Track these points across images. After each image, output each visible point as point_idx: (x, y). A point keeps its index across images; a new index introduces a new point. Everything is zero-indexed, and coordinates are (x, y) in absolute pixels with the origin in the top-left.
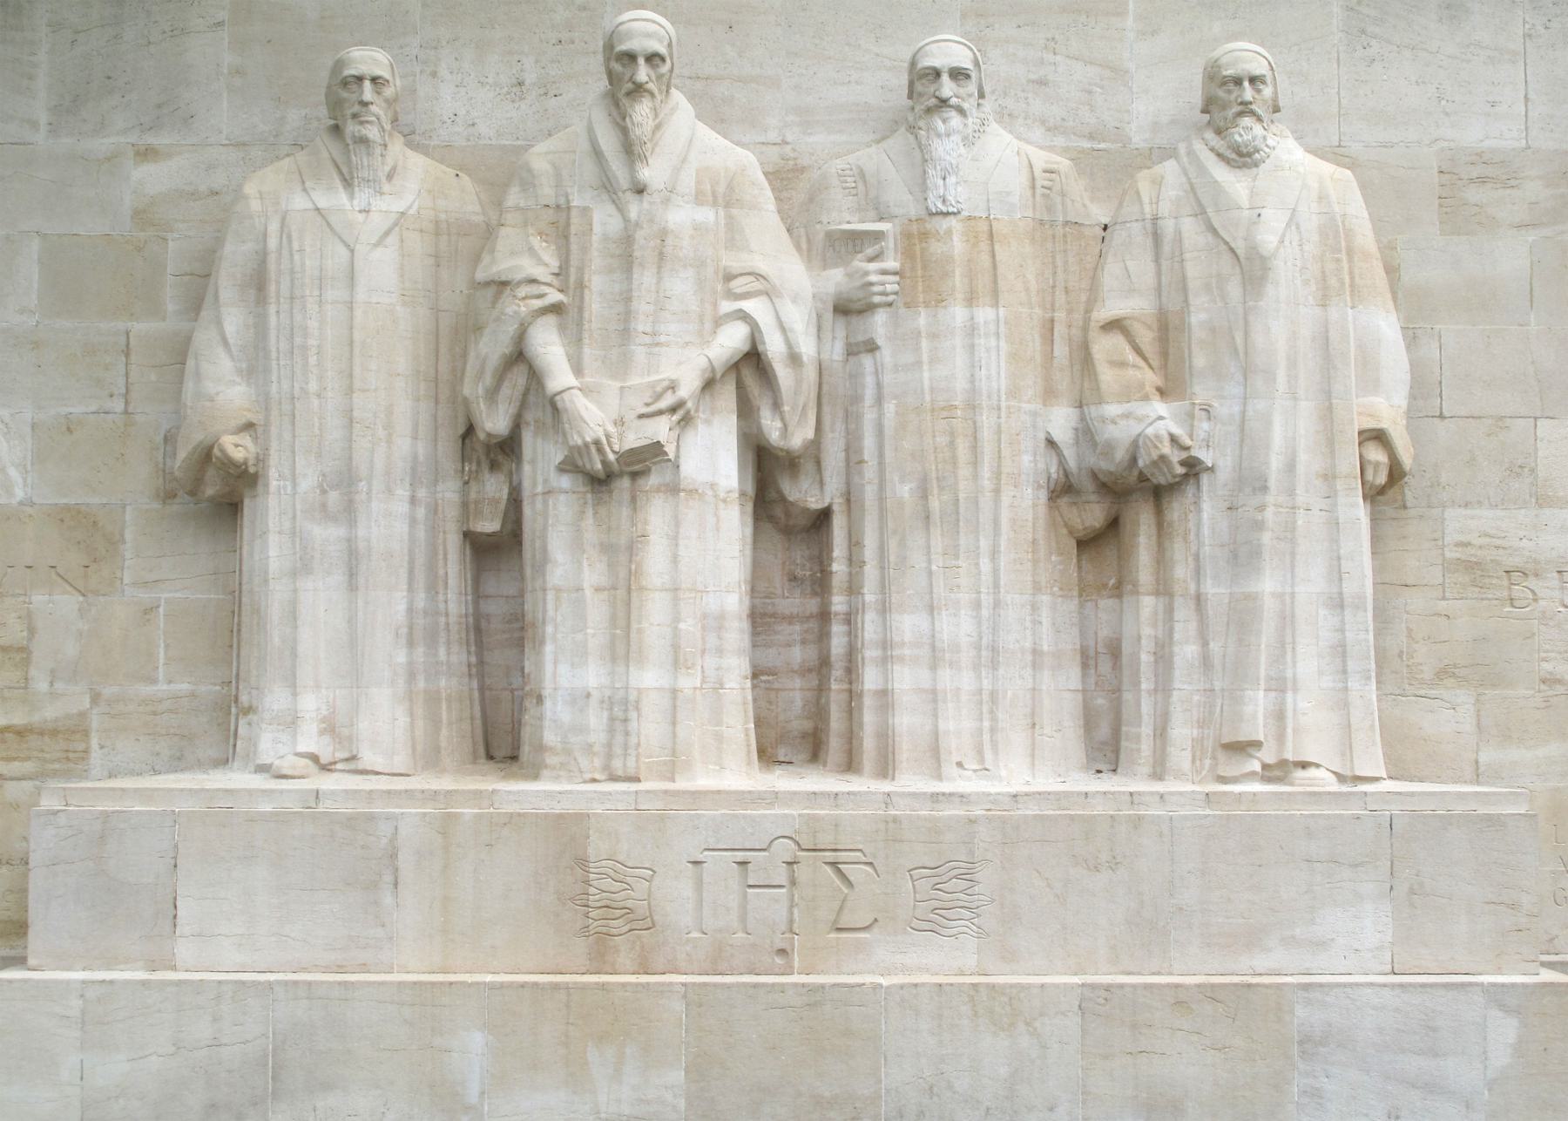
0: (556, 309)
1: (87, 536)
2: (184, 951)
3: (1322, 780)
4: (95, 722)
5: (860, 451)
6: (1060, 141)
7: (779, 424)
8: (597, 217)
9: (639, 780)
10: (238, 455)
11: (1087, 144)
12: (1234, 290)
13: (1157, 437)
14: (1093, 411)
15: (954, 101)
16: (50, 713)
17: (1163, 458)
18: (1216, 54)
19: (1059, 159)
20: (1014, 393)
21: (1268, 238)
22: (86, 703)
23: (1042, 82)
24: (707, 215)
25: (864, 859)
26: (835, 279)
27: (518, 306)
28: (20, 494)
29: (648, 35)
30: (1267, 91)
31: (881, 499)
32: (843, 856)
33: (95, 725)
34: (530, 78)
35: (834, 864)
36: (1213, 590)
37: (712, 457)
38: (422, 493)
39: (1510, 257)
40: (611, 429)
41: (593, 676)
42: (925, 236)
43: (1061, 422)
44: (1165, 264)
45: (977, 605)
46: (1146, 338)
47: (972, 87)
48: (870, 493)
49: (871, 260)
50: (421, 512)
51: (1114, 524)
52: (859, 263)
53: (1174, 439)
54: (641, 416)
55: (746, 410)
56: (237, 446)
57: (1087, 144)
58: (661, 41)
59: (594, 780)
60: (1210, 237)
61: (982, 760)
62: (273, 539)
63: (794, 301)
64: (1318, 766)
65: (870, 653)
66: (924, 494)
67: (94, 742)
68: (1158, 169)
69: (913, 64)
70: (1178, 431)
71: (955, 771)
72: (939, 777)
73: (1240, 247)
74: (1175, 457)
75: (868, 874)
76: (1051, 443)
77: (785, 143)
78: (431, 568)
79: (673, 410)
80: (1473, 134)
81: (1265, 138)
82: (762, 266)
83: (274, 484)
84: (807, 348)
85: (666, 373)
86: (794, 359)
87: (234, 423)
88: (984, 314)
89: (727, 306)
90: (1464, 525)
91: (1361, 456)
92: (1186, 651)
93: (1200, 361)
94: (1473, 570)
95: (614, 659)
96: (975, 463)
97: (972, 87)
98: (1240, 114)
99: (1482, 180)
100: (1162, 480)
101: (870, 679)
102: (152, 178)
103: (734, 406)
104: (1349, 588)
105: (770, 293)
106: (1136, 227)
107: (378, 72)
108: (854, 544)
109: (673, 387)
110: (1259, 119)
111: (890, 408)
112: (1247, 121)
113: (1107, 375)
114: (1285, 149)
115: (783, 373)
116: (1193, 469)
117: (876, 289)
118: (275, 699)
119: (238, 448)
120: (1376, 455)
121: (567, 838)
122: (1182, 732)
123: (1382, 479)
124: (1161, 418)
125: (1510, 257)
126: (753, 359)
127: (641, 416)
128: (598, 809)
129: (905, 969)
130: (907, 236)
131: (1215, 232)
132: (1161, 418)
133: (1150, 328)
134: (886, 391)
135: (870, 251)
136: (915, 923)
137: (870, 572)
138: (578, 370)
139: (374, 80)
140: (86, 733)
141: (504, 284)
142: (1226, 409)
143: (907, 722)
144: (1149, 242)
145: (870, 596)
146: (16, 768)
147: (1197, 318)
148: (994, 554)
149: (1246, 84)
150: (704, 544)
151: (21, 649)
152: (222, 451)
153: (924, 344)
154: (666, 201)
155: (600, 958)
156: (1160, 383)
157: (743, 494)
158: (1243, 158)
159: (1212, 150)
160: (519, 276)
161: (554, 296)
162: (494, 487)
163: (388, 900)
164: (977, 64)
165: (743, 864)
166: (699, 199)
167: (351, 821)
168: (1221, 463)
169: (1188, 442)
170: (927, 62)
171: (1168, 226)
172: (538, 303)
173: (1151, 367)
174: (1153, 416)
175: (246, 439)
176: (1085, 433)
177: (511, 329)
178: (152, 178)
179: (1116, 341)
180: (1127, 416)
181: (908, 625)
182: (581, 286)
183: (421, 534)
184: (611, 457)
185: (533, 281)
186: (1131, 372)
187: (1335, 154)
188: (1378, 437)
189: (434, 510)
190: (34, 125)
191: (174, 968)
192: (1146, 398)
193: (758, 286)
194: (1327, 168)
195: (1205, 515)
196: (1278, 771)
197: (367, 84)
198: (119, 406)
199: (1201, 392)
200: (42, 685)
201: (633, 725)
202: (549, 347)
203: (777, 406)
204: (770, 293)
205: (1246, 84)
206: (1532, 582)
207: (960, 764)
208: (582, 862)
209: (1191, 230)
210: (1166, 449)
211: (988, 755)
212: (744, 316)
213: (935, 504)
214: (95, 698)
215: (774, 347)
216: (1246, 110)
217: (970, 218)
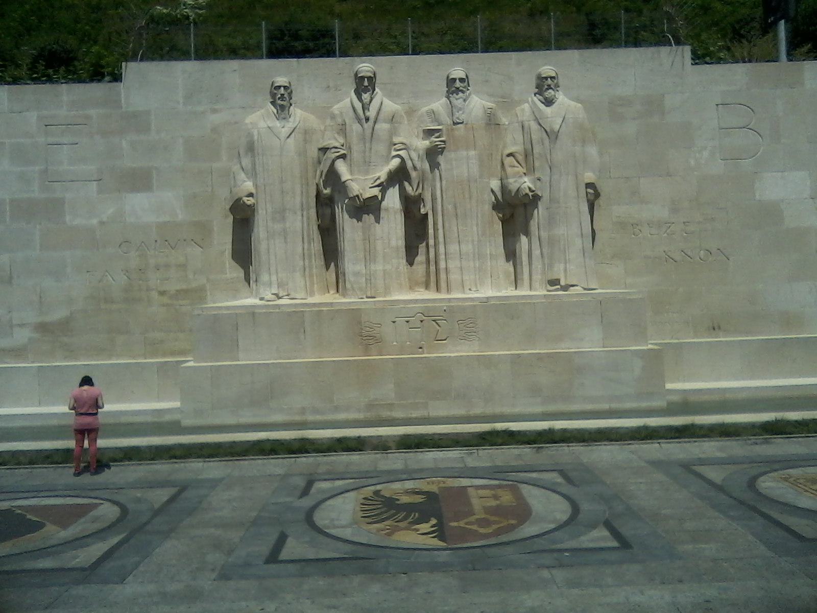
0: (343, 157)
1: (201, 232)
2: (241, 355)
3: (578, 290)
4: (208, 287)
5: (436, 195)
6: (492, 99)
7: (411, 188)
8: (354, 127)
9: (375, 298)
10: (249, 203)
11: (502, 100)
12: (547, 141)
13: (525, 188)
14: (505, 181)
15: (461, 88)
16: (194, 285)
17: (527, 194)
18: (540, 70)
19: (492, 105)
21: (557, 127)
22: (205, 281)
23: (487, 81)
25: (444, 319)
26: (426, 143)
27: (332, 155)
28: (180, 217)
29: (368, 71)
30: (555, 81)
31: (442, 211)
33: (208, 288)
34: (331, 85)
35: (434, 321)
36: (544, 234)
37: (393, 200)
38: (305, 213)
39: (631, 128)
40: (361, 191)
41: (360, 267)
42: (452, 130)
43: (495, 184)
44: (525, 136)
45: (473, 241)
46: (521, 158)
47: (466, 84)
48: (439, 208)
49: (436, 138)
50: (305, 219)
51: (512, 216)
52: (433, 139)
53: (530, 189)
54: (371, 188)
56: (248, 200)
57: (502, 100)
58: (371, 72)
59: (362, 298)
60: (539, 127)
61: (477, 288)
62: (261, 229)
63: (414, 150)
64: (577, 286)
65: (442, 257)
66: (456, 208)
67: (209, 294)
68: (522, 107)
69: (448, 77)
70: (531, 186)
71: (469, 291)
72: (464, 293)
73: (548, 130)
74: (530, 194)
75: (445, 323)
76: (492, 191)
77: (409, 103)
78: (309, 236)
79: (378, 186)
81: (555, 96)
82: (405, 141)
83: (260, 212)
84: (418, 165)
85: (377, 175)
86: (415, 168)
87: (246, 194)
88: (472, 153)
89: (394, 153)
90: (620, 211)
91: (586, 192)
92: (536, 252)
93: (537, 164)
94: (622, 225)
95: (366, 261)
96: (470, 198)
97: (466, 84)
98: (547, 89)
100: (526, 201)
101: (442, 265)
102: (216, 118)
104: (584, 231)
105: (406, 148)
106: (517, 124)
107: (286, 85)
108: (435, 224)
109: (379, 178)
110: (554, 90)
111: (444, 182)
112: (550, 91)
113: (509, 170)
114: (561, 98)
115: (413, 174)
116: (536, 198)
117: (439, 146)
118: (265, 277)
119: (250, 201)
121: (354, 316)
122: (537, 277)
123: (592, 198)
124: (525, 182)
125: (631, 128)
127: (371, 188)
128: (363, 307)
129: (457, 351)
130: (448, 130)
131: (540, 125)
132: (525, 182)
133: (522, 155)
134: (443, 178)
135: (437, 135)
136: (460, 337)
137: (441, 231)
138: (351, 174)
139: (285, 87)
140: (206, 291)
141: (328, 148)
142: (546, 179)
143: (454, 277)
144: (521, 129)
145: (441, 239)
146: (184, 302)
147: (536, 151)
148: (477, 225)
149: (549, 79)
150: (391, 227)
151: (184, 265)
152: (244, 202)
153: (454, 163)
154: (375, 122)
155: (367, 352)
156: (525, 171)
157: (401, 210)
158: (549, 102)
159: (539, 100)
160: (331, 146)
161: (342, 152)
162: (328, 211)
163: (303, 337)
164: (467, 76)
165: (407, 322)
167: (289, 314)
168: (544, 195)
169: (534, 189)
170: (451, 77)
171: (526, 124)
172: (338, 154)
173: (523, 168)
174: (523, 181)
175: (250, 198)
176: (503, 188)
177: (329, 163)
178: (216, 119)
179: (511, 158)
180: (515, 182)
181: (453, 248)
182: (350, 148)
183: (305, 225)
184: (362, 200)
185: (336, 148)
186: (516, 169)
187: (578, 100)
189: (308, 218)
190: (178, 103)
191: (239, 361)
192: (521, 177)
193: (403, 147)
194: (573, 103)
195: (540, 213)
196: (566, 288)
197: (282, 88)
198: (210, 189)
199: (537, 175)
200: (191, 276)
201: (373, 281)
202: (342, 167)
203: (410, 184)
204: (406, 148)
205: (549, 79)
206: (639, 227)
207: (470, 290)
208: (360, 323)
209: (534, 126)
210: (527, 191)
211: (478, 285)
212: (398, 156)
213: (459, 211)
214: (208, 280)
215: (409, 164)
216: (549, 87)
217: (466, 124)
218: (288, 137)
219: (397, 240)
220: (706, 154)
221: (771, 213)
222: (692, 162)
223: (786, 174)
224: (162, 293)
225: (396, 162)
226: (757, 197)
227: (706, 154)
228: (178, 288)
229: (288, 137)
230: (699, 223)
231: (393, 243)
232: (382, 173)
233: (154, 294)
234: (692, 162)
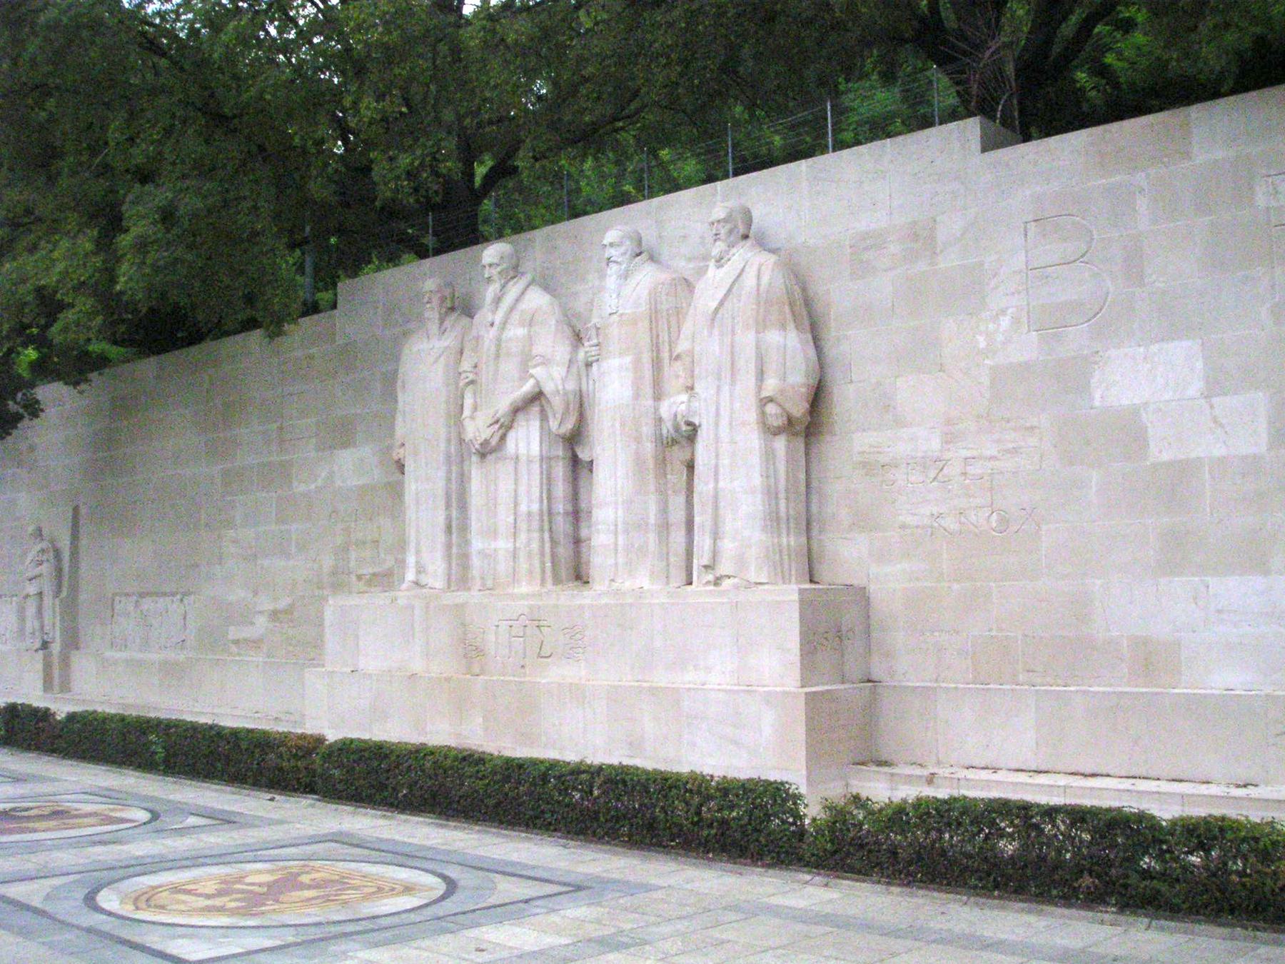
0: (472, 382)
20: (637, 396)
24: (521, 332)
32: (542, 623)
37: (527, 440)
55: (544, 417)
80: (864, 223)
94: (868, 467)
99: (866, 249)
103: (538, 416)
120: (771, 409)
126: (537, 397)
161: (471, 377)
166: (522, 324)
188: (771, 400)
215: (548, 388)
218: (435, 362)
219: (530, 501)
220: (1005, 322)
221: (1129, 431)
222: (982, 342)
223: (1154, 348)
224: (359, 578)
225: (528, 387)
226: (1097, 403)
227: (1005, 322)
228: (375, 570)
229: (435, 362)
230: (992, 458)
231: (523, 508)
232: (503, 404)
233: (354, 578)
234: (982, 342)
